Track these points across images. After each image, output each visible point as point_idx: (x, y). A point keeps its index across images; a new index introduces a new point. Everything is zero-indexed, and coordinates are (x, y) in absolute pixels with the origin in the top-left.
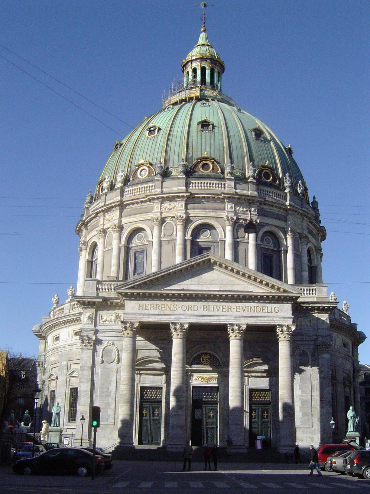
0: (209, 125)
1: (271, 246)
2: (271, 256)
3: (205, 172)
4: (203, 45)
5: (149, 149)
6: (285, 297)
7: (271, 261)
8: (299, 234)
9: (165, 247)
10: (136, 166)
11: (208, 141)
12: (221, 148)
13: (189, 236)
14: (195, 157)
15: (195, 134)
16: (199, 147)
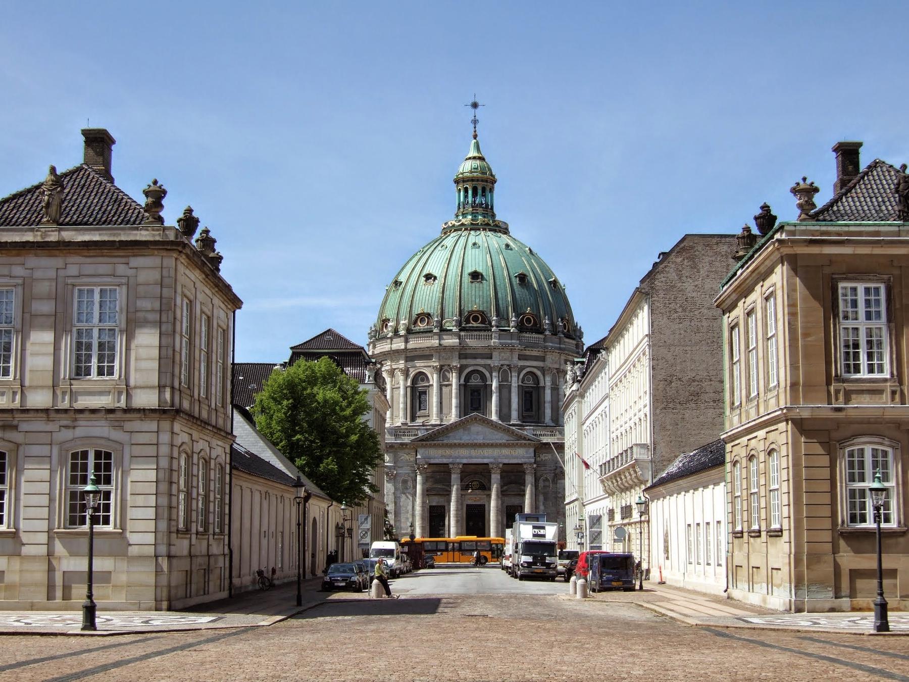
0: (479, 275)
1: (530, 383)
2: (532, 392)
3: (475, 324)
4: (474, 158)
5: (427, 297)
6: (530, 444)
7: (531, 396)
8: (557, 369)
9: (444, 389)
10: (417, 315)
11: (477, 294)
12: (489, 300)
13: (462, 381)
14: (466, 309)
15: (466, 287)
16: (470, 299)
